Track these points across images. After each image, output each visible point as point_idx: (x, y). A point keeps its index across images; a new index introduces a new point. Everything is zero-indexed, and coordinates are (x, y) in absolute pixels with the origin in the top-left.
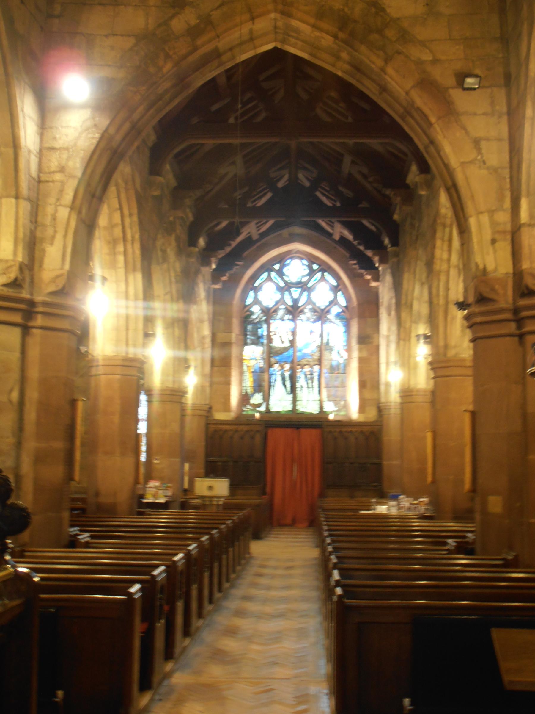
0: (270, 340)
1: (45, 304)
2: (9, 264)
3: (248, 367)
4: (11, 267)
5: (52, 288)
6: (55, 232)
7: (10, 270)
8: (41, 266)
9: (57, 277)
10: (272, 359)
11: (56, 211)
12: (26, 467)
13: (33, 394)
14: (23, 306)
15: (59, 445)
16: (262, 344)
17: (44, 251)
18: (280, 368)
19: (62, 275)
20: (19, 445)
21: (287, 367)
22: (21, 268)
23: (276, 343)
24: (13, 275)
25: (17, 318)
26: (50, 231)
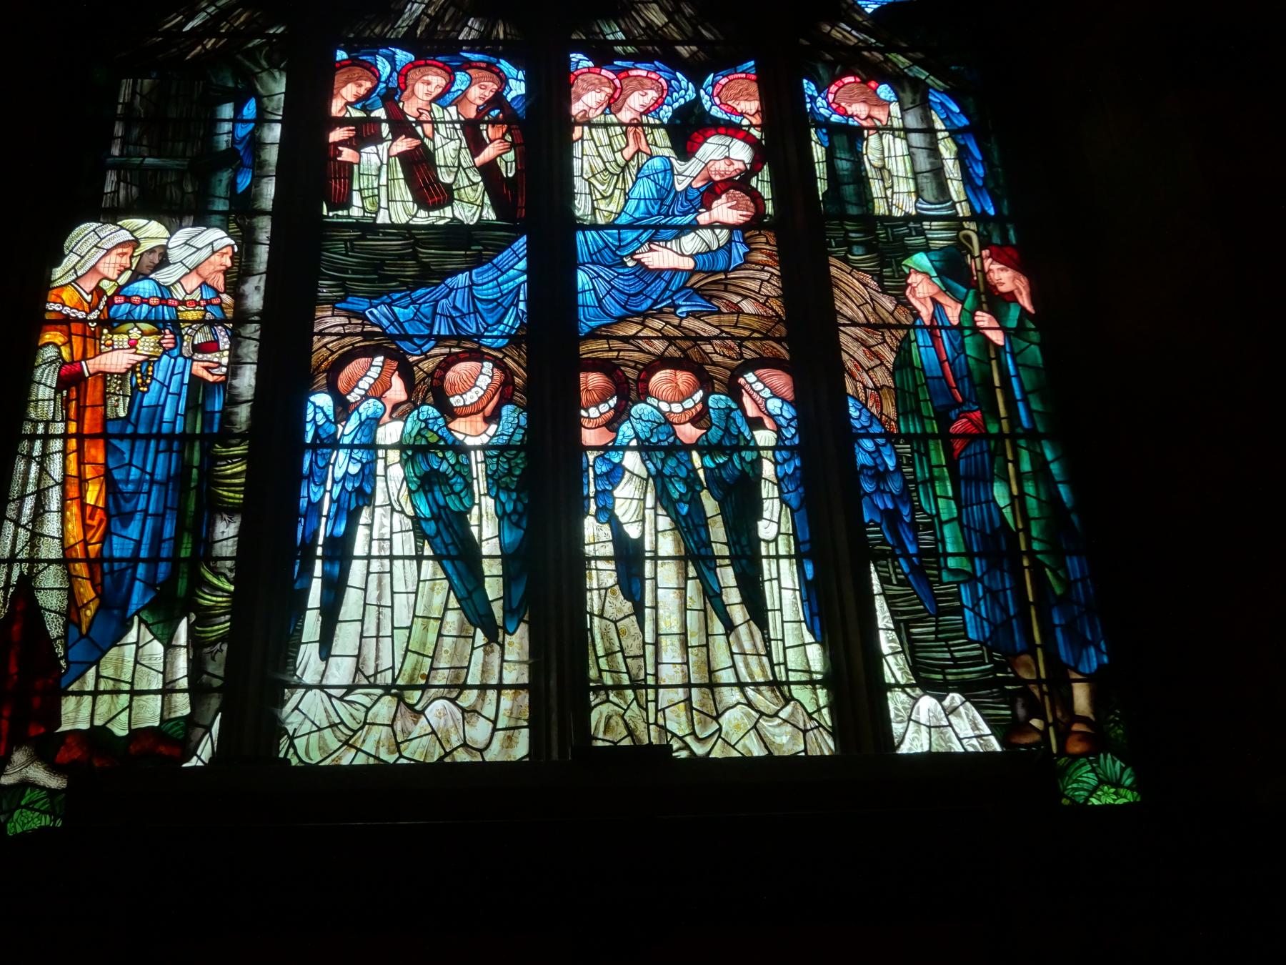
0: (314, 172)
3: (71, 380)
10: (329, 321)
16: (240, 215)
18: (397, 391)
21: (474, 382)
23: (378, 190)
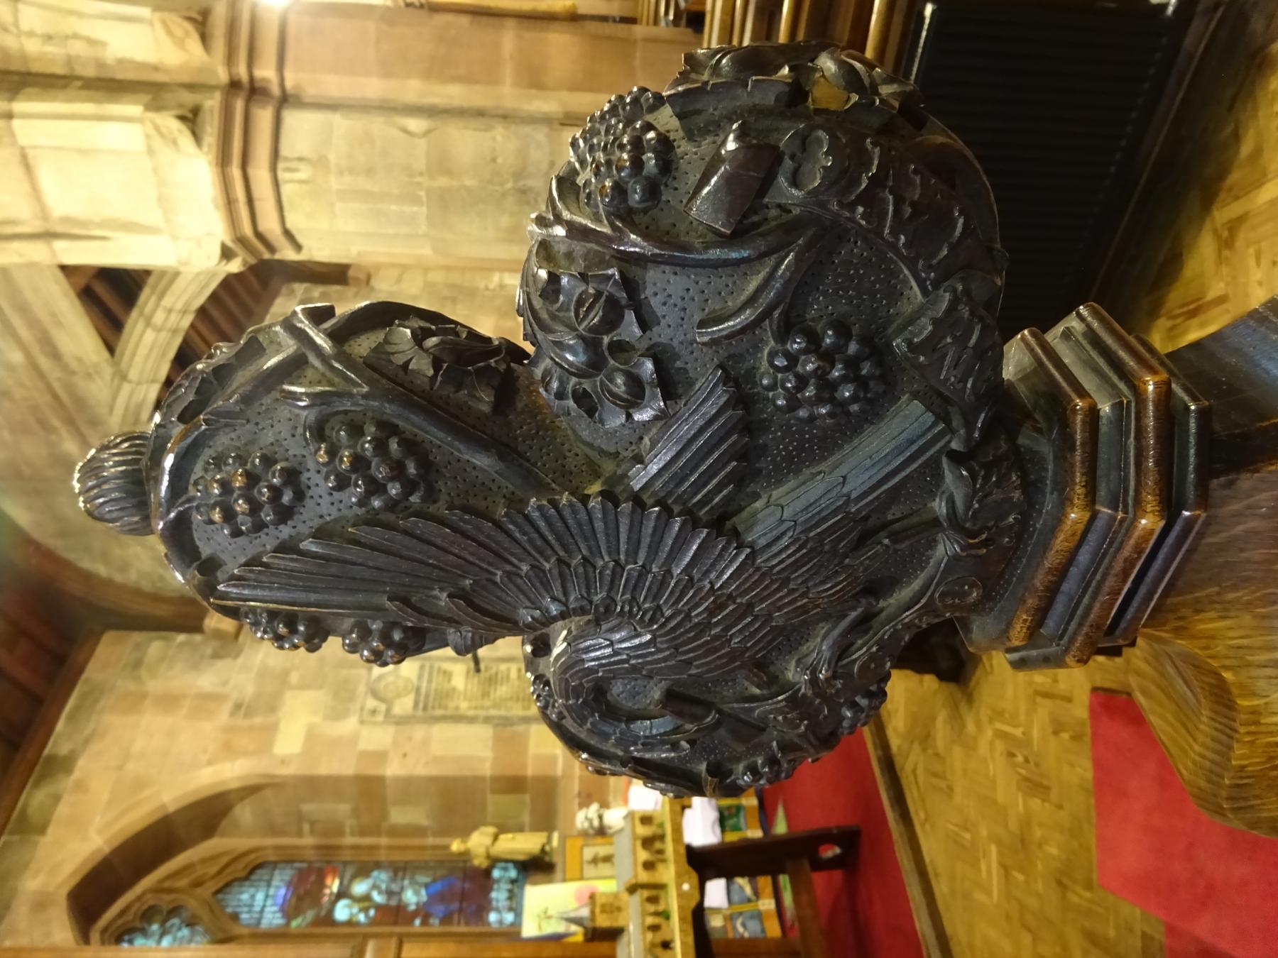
1: (230, 59)
2: (153, 132)
4: (157, 128)
5: (195, 45)
6: (76, 36)
7: (164, 130)
8: (156, 68)
9: (170, 33)
11: (31, 34)
12: (548, 105)
13: (413, 89)
14: (239, 105)
15: (509, 39)
17: (121, 62)
19: (164, 23)
20: (507, 117)
22: (155, 106)
24: (169, 122)
25: (264, 117)
26: (77, 48)
